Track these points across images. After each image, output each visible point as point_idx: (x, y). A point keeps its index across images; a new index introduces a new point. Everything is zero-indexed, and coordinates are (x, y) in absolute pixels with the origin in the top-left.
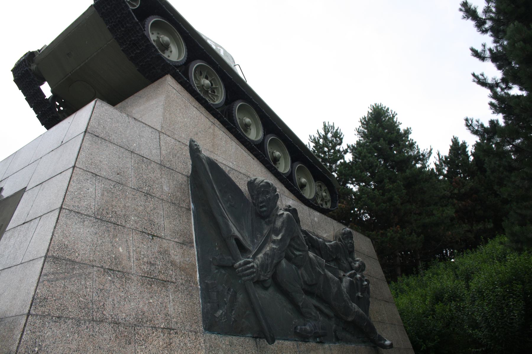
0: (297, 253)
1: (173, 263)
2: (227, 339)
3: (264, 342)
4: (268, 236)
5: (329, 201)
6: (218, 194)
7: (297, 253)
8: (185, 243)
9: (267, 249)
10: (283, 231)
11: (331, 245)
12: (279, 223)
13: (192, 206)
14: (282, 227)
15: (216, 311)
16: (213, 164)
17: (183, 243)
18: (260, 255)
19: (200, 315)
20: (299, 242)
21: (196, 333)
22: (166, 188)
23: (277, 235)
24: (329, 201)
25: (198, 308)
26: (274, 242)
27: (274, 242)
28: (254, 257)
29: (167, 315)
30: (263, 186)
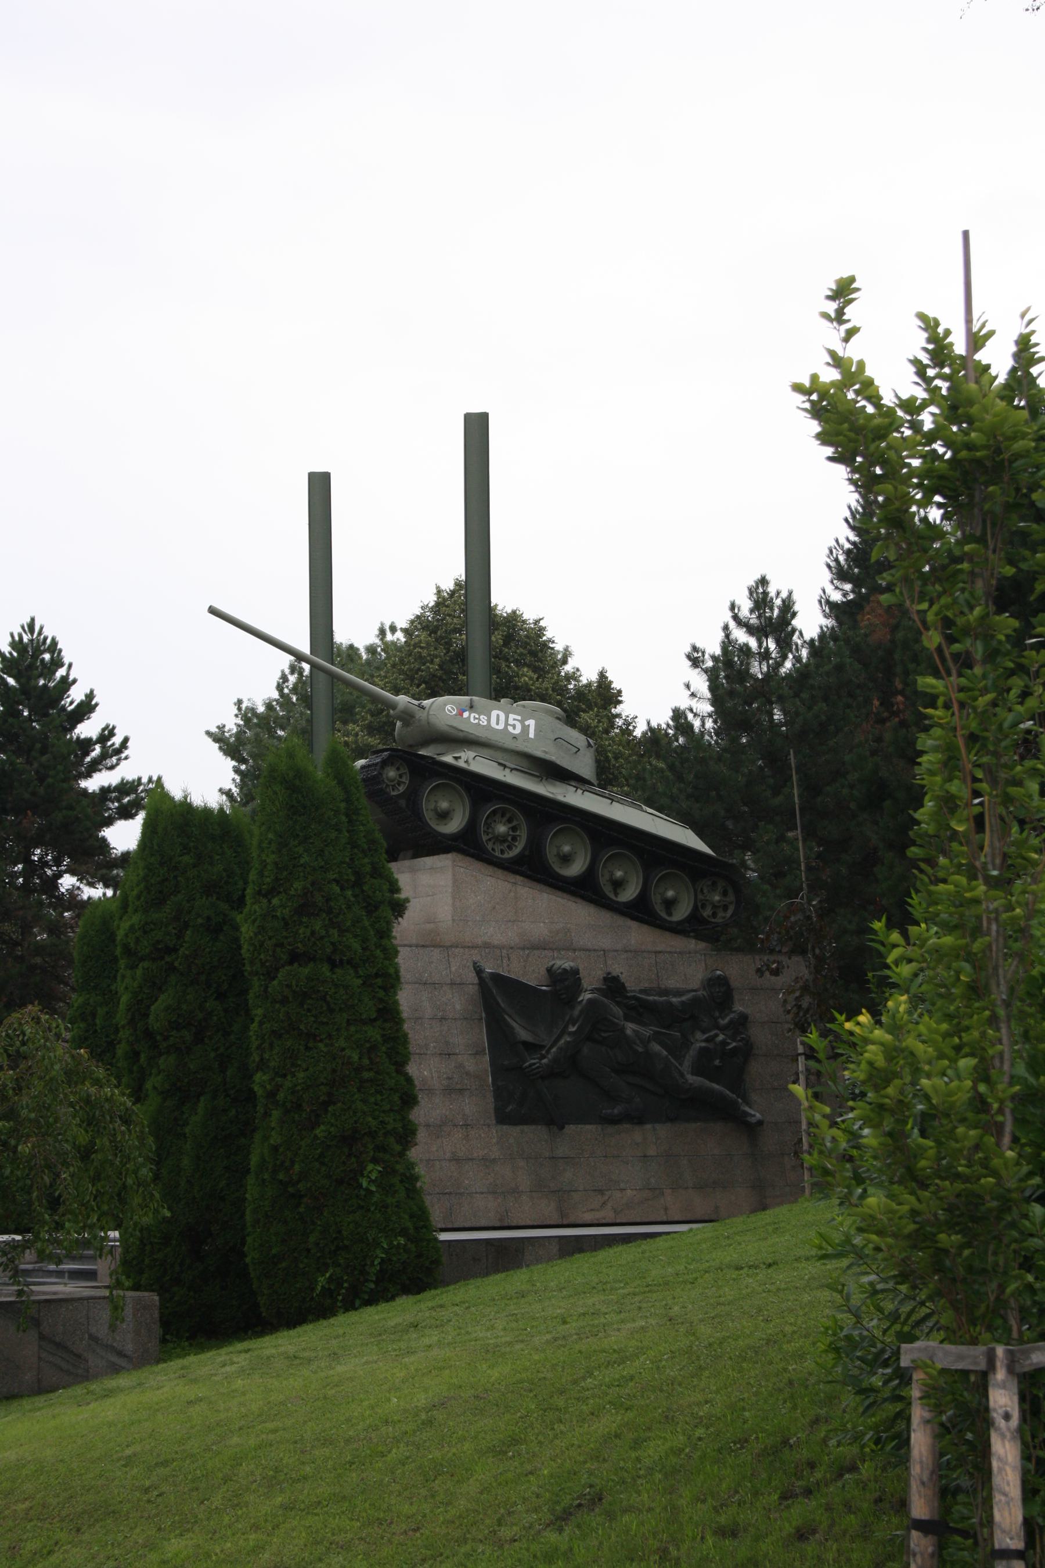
1: (467, 1073)
2: (519, 1128)
4: (566, 1027)
5: (731, 903)
6: (503, 1005)
8: (478, 1053)
9: (562, 1041)
11: (683, 1003)
12: (576, 1012)
13: (484, 1015)
16: (497, 978)
17: (476, 1054)
18: (554, 1050)
19: (492, 1111)
21: (489, 1126)
22: (458, 1007)
23: (574, 1025)
24: (731, 903)
25: (491, 1106)
26: (570, 1034)
27: (570, 1034)
28: (548, 1052)
29: (464, 1115)
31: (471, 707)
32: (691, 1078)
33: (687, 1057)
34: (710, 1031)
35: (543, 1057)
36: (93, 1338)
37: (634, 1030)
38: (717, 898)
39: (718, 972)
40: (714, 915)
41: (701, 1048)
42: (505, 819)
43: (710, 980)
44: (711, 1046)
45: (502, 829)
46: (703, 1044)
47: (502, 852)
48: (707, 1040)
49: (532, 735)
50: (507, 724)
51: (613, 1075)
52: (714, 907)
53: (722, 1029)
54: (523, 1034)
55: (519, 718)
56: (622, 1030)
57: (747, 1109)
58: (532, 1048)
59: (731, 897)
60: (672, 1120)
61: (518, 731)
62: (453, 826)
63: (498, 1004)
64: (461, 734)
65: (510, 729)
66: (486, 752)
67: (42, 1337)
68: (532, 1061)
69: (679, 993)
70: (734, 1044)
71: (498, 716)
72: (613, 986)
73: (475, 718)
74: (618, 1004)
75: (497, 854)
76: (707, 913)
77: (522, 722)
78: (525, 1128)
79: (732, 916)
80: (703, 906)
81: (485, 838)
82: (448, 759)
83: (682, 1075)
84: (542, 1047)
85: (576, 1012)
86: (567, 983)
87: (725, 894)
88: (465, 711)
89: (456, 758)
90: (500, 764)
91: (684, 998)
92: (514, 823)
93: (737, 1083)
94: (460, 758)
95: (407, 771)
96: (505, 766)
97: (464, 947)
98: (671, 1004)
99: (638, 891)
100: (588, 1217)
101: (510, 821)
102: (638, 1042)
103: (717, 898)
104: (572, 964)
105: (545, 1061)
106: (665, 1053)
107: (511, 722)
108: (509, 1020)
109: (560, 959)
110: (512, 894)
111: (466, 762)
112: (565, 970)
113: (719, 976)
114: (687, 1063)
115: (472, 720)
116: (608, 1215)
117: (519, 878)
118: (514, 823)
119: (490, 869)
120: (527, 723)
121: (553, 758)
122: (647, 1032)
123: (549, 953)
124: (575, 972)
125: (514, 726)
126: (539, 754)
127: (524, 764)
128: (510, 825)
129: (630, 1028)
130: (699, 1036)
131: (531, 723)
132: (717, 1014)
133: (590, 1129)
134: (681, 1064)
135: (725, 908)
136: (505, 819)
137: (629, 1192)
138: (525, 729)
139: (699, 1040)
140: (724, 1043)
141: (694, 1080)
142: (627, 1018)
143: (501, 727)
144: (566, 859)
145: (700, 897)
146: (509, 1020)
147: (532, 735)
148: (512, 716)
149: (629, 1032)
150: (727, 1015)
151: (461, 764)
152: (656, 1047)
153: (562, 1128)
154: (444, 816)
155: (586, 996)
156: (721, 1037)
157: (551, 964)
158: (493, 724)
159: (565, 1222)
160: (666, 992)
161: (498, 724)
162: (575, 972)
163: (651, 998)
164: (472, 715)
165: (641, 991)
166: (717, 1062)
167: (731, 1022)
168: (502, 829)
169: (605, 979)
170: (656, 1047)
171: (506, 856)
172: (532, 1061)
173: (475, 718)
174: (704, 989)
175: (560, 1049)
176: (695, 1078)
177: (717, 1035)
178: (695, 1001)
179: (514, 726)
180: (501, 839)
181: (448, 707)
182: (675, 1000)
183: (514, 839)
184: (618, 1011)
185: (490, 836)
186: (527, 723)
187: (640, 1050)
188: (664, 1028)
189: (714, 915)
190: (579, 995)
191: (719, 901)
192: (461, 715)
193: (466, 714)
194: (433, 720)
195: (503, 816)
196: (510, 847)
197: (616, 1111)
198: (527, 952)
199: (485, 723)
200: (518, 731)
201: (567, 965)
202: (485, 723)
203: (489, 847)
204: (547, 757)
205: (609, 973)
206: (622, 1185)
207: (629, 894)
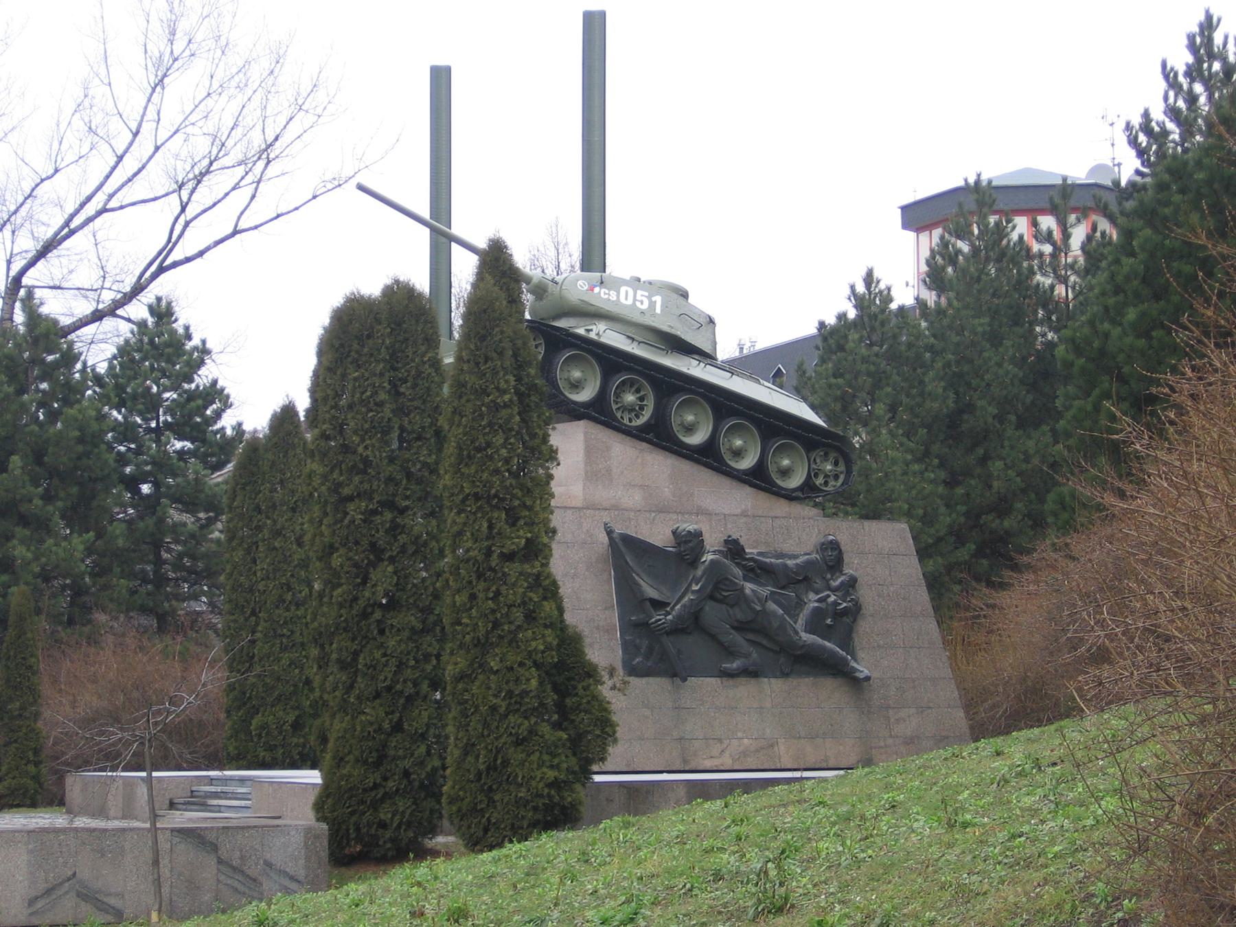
0: (726, 594)
2: (644, 680)
3: (677, 680)
4: (690, 585)
5: (841, 473)
7: (726, 594)
9: (686, 599)
10: (703, 579)
12: (699, 572)
14: (702, 576)
15: (634, 660)
16: (628, 540)
17: (606, 609)
18: (678, 607)
20: (727, 583)
24: (841, 473)
26: (693, 592)
28: (672, 609)
30: (685, 535)
31: (602, 283)
32: (807, 637)
33: (801, 615)
34: (822, 592)
35: (668, 613)
36: (268, 864)
37: (753, 590)
38: (829, 467)
39: (831, 537)
40: (826, 483)
41: (816, 609)
42: (633, 389)
43: (823, 544)
44: (823, 605)
45: (630, 398)
46: (816, 604)
47: (630, 420)
48: (819, 601)
49: (658, 310)
50: (635, 299)
51: (732, 631)
52: (826, 476)
53: (834, 590)
54: (652, 593)
55: (647, 294)
56: (742, 589)
57: (855, 665)
58: (658, 605)
59: (842, 467)
60: (785, 675)
61: (645, 306)
62: (584, 396)
63: (627, 563)
64: (592, 309)
65: (638, 304)
66: (618, 326)
67: (220, 861)
68: (657, 617)
69: (795, 557)
70: (845, 605)
71: (627, 292)
72: (734, 549)
73: (605, 294)
74: (738, 564)
75: (626, 421)
76: (819, 481)
77: (649, 298)
78: (651, 680)
79: (842, 484)
80: (816, 475)
81: (614, 407)
82: (581, 331)
83: (796, 633)
84: (668, 604)
85: (699, 572)
86: (691, 545)
87: (836, 464)
88: (595, 286)
89: (588, 331)
90: (629, 337)
91: (798, 561)
92: (642, 393)
93: (847, 643)
94: (592, 330)
95: (542, 341)
96: (633, 339)
97: (595, 509)
98: (786, 566)
99: (755, 460)
100: (708, 764)
101: (638, 391)
102: (756, 601)
103: (829, 467)
104: (696, 527)
105: (670, 617)
106: (781, 612)
107: (639, 297)
108: (636, 577)
109: (686, 522)
110: (639, 460)
111: (598, 334)
112: (689, 532)
113: (831, 542)
114: (800, 624)
115: (602, 295)
116: (727, 762)
117: (645, 445)
118: (642, 393)
119: (620, 436)
120: (654, 299)
121: (679, 333)
122: (765, 591)
123: (675, 516)
124: (698, 535)
125: (642, 302)
126: (665, 328)
127: (651, 338)
128: (638, 395)
129: (749, 587)
130: (812, 596)
131: (658, 299)
132: (829, 576)
133: (713, 682)
134: (795, 623)
135: (836, 477)
136: (633, 389)
137: (746, 741)
138: (652, 305)
139: (812, 601)
140: (836, 604)
141: (807, 637)
142: (746, 578)
143: (630, 302)
144: (690, 429)
145: (813, 466)
146: (636, 577)
147: (658, 310)
148: (639, 292)
149: (747, 591)
150: (837, 579)
151: (593, 335)
152: (772, 606)
153: (684, 680)
154: (576, 386)
155: (708, 557)
156: (833, 598)
157: (675, 526)
158: (622, 299)
159: (687, 768)
160: (781, 555)
161: (626, 299)
162: (698, 535)
163: (768, 560)
164: (603, 290)
165: (760, 554)
166: (829, 621)
167: (842, 583)
168: (630, 398)
169: (726, 542)
170: (772, 606)
171: (634, 424)
172: (657, 617)
173: (605, 294)
174: (817, 552)
175: (684, 606)
176: (808, 635)
177: (829, 596)
178: (809, 563)
179: (642, 302)
180: (631, 410)
181: (580, 282)
182: (790, 562)
183: (642, 408)
184: (738, 572)
185: (619, 405)
186: (654, 299)
187: (758, 608)
188: (780, 589)
189: (826, 483)
190: (702, 555)
191: (831, 471)
192: (592, 290)
193: (597, 290)
194: (567, 294)
195: (631, 386)
196: (637, 417)
197: (735, 665)
198: (653, 514)
199: (615, 299)
200: (645, 306)
201: (691, 528)
202: (615, 299)
203: (619, 415)
204: (673, 331)
205: (729, 536)
206: (740, 735)
207: (747, 463)
